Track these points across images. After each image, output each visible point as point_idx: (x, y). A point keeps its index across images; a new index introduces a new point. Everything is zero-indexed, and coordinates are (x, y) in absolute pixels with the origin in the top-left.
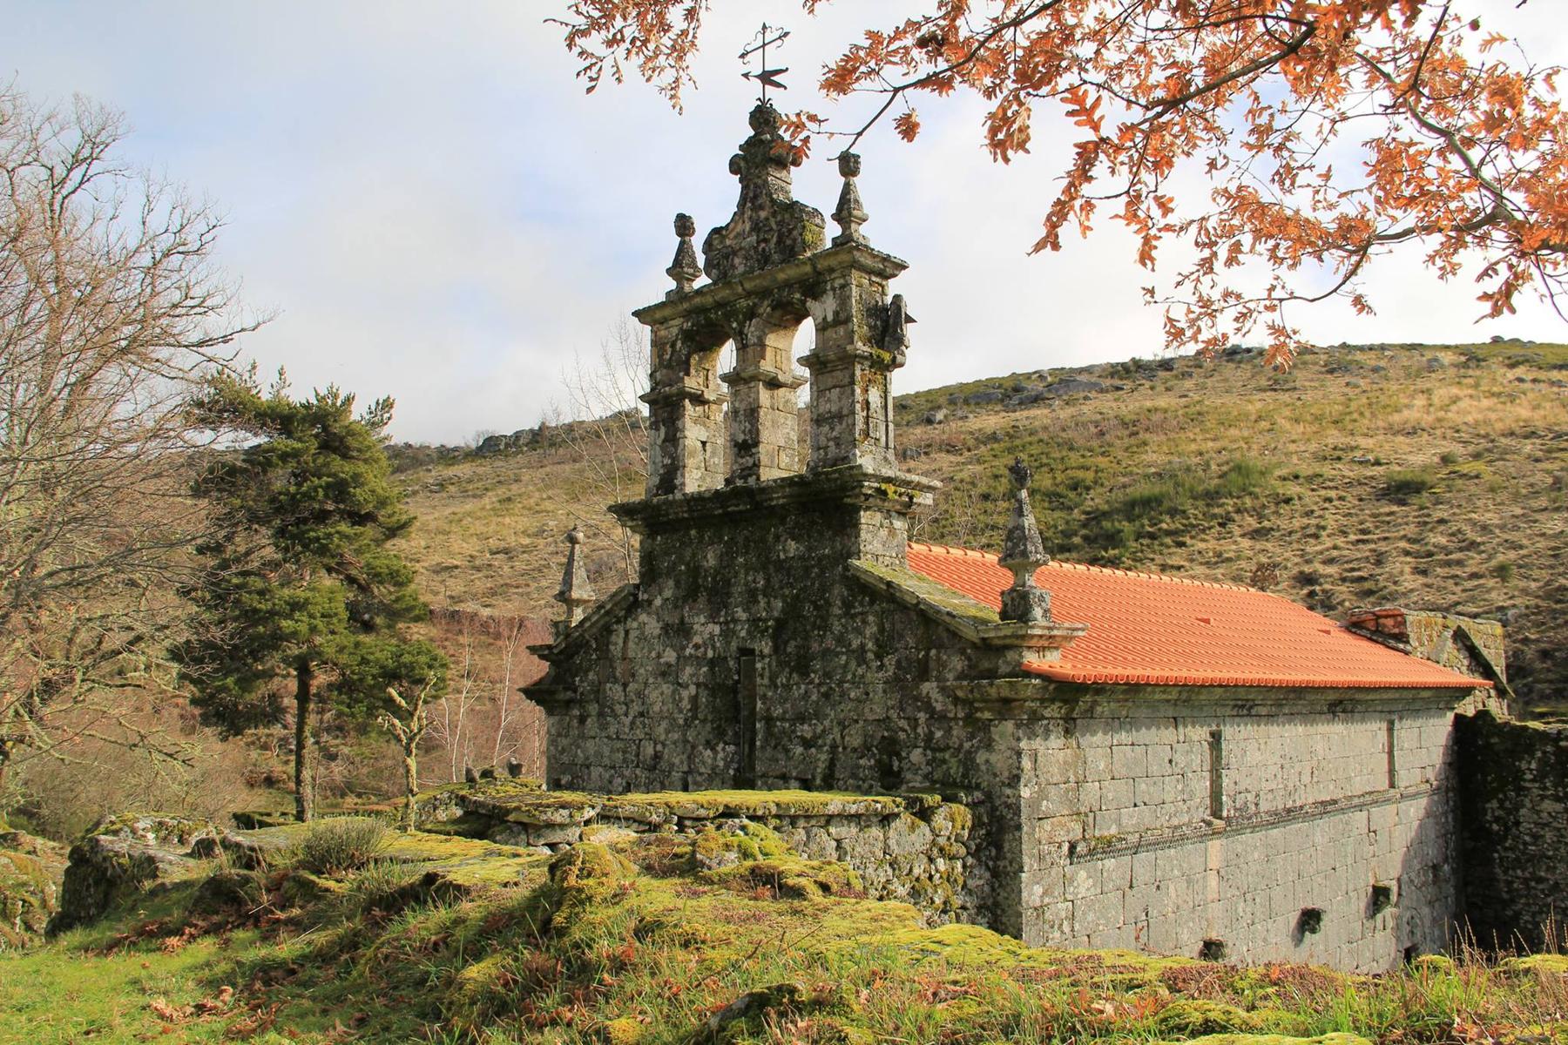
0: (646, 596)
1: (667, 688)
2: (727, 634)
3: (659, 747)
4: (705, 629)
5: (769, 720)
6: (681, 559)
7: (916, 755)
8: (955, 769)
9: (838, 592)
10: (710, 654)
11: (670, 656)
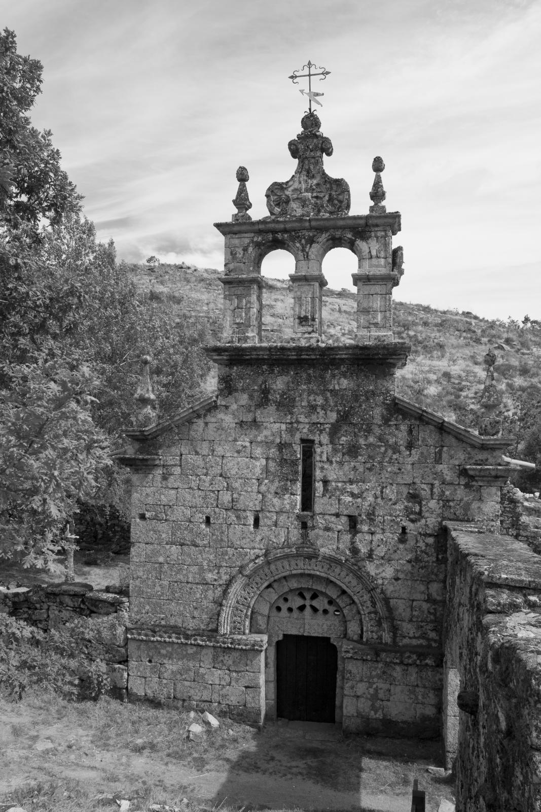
0: (223, 403)
2: (291, 431)
4: (273, 425)
5: (326, 482)
6: (254, 382)
7: (433, 504)
10: (278, 441)
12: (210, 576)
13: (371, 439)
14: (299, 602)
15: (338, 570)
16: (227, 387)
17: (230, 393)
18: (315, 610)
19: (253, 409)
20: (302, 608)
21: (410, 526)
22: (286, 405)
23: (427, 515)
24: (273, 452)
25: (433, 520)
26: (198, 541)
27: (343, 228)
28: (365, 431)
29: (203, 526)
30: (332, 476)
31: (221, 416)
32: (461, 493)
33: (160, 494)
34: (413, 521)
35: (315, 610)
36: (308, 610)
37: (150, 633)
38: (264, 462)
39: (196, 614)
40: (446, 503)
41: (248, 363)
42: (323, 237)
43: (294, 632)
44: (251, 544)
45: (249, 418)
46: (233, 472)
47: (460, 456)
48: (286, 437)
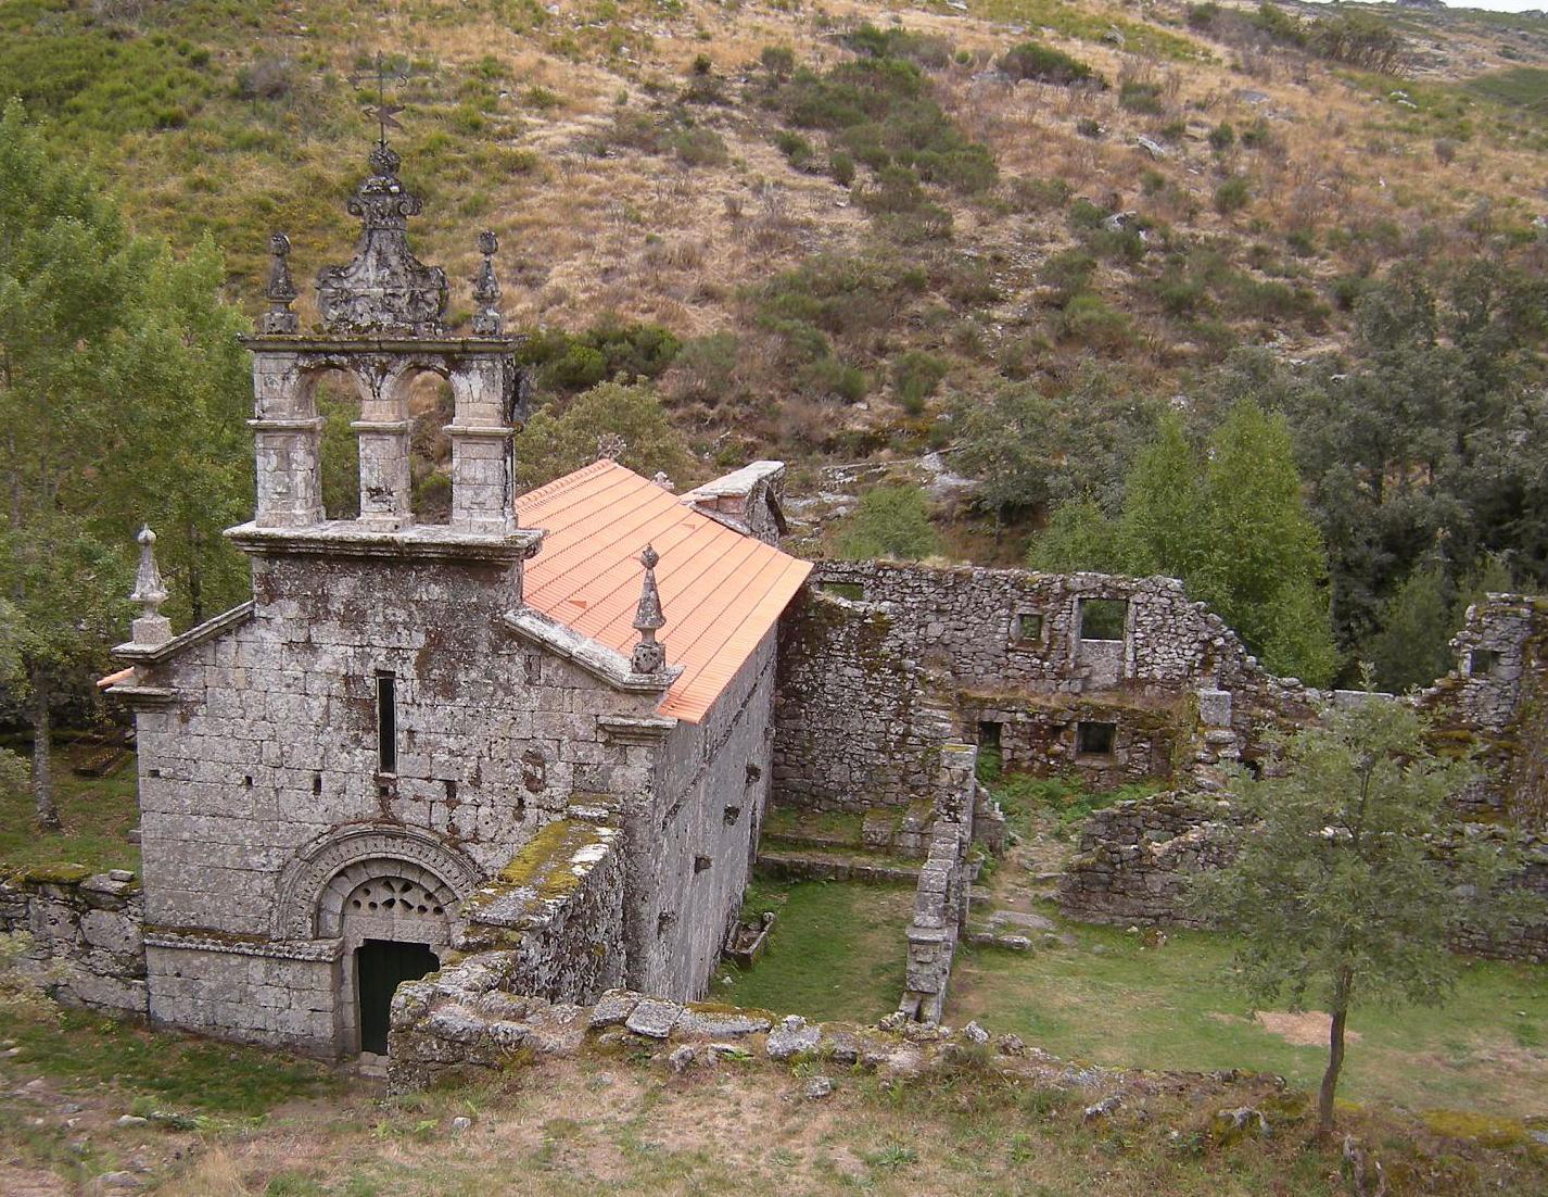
0: (263, 614)
1: (294, 699)
2: (363, 658)
3: (285, 748)
4: (335, 650)
5: (411, 733)
7: (560, 768)
9: (484, 636)
10: (343, 671)
12: (256, 860)
13: (473, 675)
14: (385, 895)
15: (432, 855)
17: (271, 601)
19: (306, 624)
20: (390, 903)
21: (530, 798)
22: (353, 618)
23: (552, 782)
24: (337, 687)
25: (561, 790)
26: (237, 812)
27: (431, 353)
28: (465, 661)
29: (243, 790)
30: (420, 726)
31: (262, 632)
32: (598, 755)
33: (180, 743)
34: (535, 791)
37: (175, 936)
38: (324, 700)
39: (239, 910)
40: (578, 767)
41: (299, 557)
42: (402, 365)
43: (379, 935)
44: (313, 818)
45: (300, 636)
46: (282, 714)
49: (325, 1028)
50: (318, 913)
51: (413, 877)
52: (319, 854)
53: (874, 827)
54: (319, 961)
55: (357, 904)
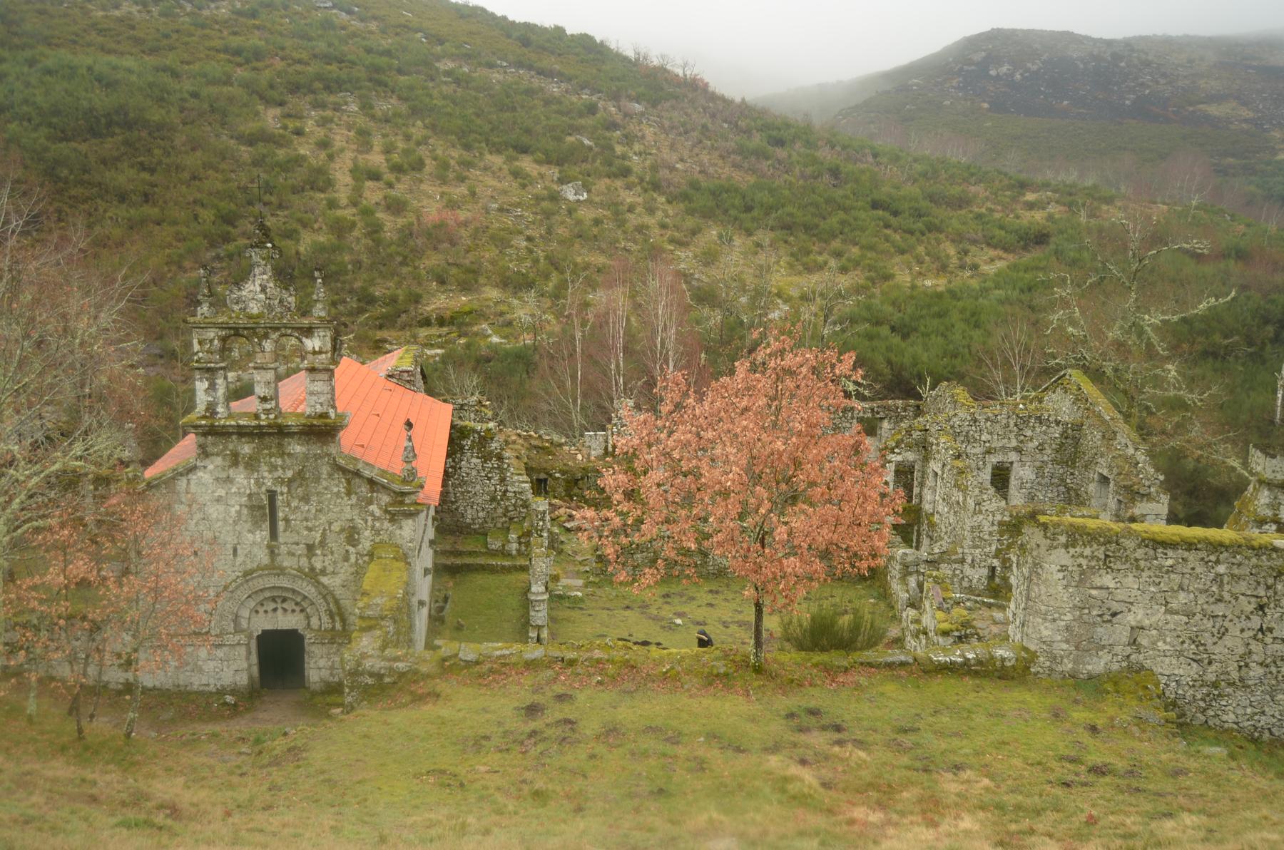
1: (221, 508)
2: (259, 483)
5: (287, 520)
7: (367, 533)
8: (386, 538)
9: (325, 470)
11: (221, 492)
16: (204, 453)
18: (285, 610)
20: (275, 610)
21: (352, 549)
31: (200, 474)
32: (386, 524)
35: (285, 610)
36: (280, 611)
38: (237, 508)
42: (275, 336)
45: (224, 475)
46: (214, 516)
47: (385, 499)
48: (254, 489)
49: (243, 680)
50: (236, 619)
51: (289, 595)
52: (237, 588)
53: (495, 544)
54: (239, 644)
55: (257, 612)
